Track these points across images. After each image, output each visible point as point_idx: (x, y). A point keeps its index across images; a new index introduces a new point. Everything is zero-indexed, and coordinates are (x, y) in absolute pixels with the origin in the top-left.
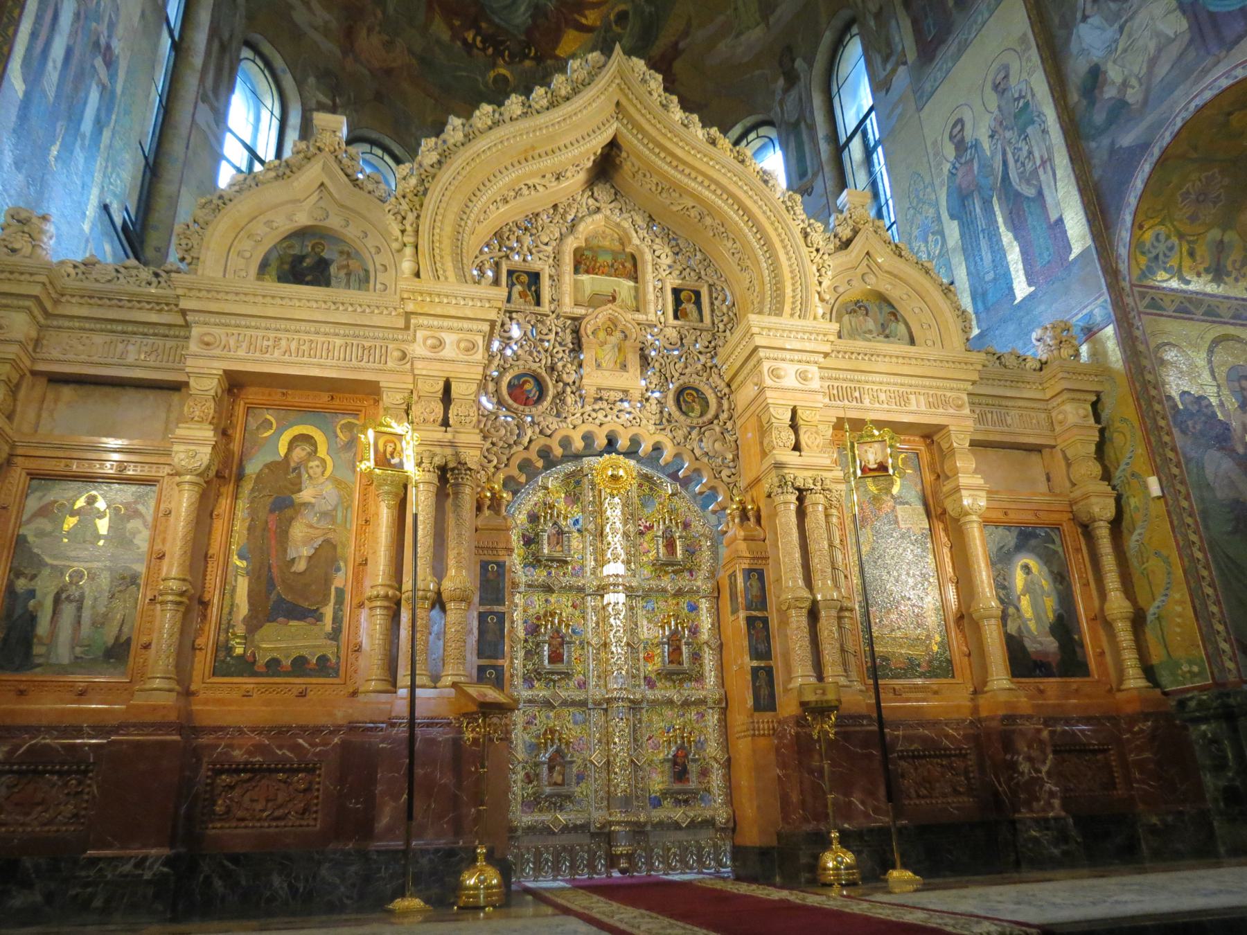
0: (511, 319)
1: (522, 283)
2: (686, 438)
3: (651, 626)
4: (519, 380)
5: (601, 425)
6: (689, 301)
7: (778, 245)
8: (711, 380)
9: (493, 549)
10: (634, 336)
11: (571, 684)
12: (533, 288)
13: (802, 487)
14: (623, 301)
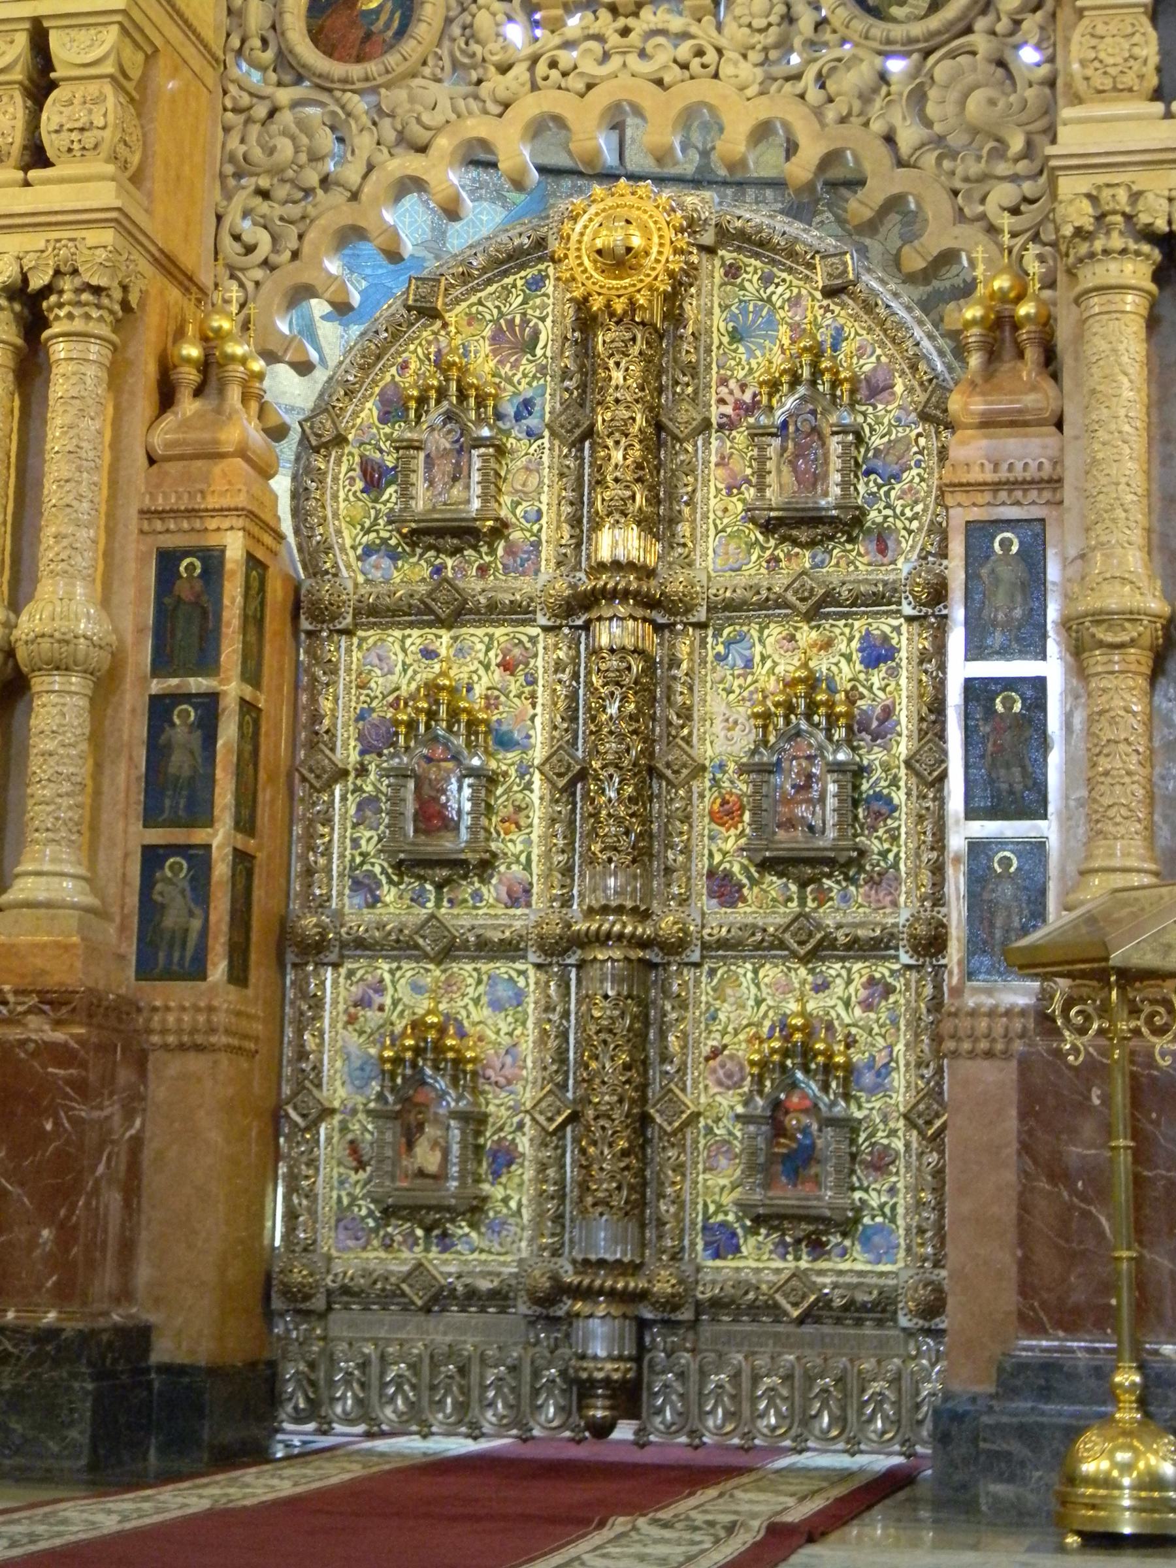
2: (866, 98)
5: (590, 87)
9: (192, 513)
11: (489, 893)
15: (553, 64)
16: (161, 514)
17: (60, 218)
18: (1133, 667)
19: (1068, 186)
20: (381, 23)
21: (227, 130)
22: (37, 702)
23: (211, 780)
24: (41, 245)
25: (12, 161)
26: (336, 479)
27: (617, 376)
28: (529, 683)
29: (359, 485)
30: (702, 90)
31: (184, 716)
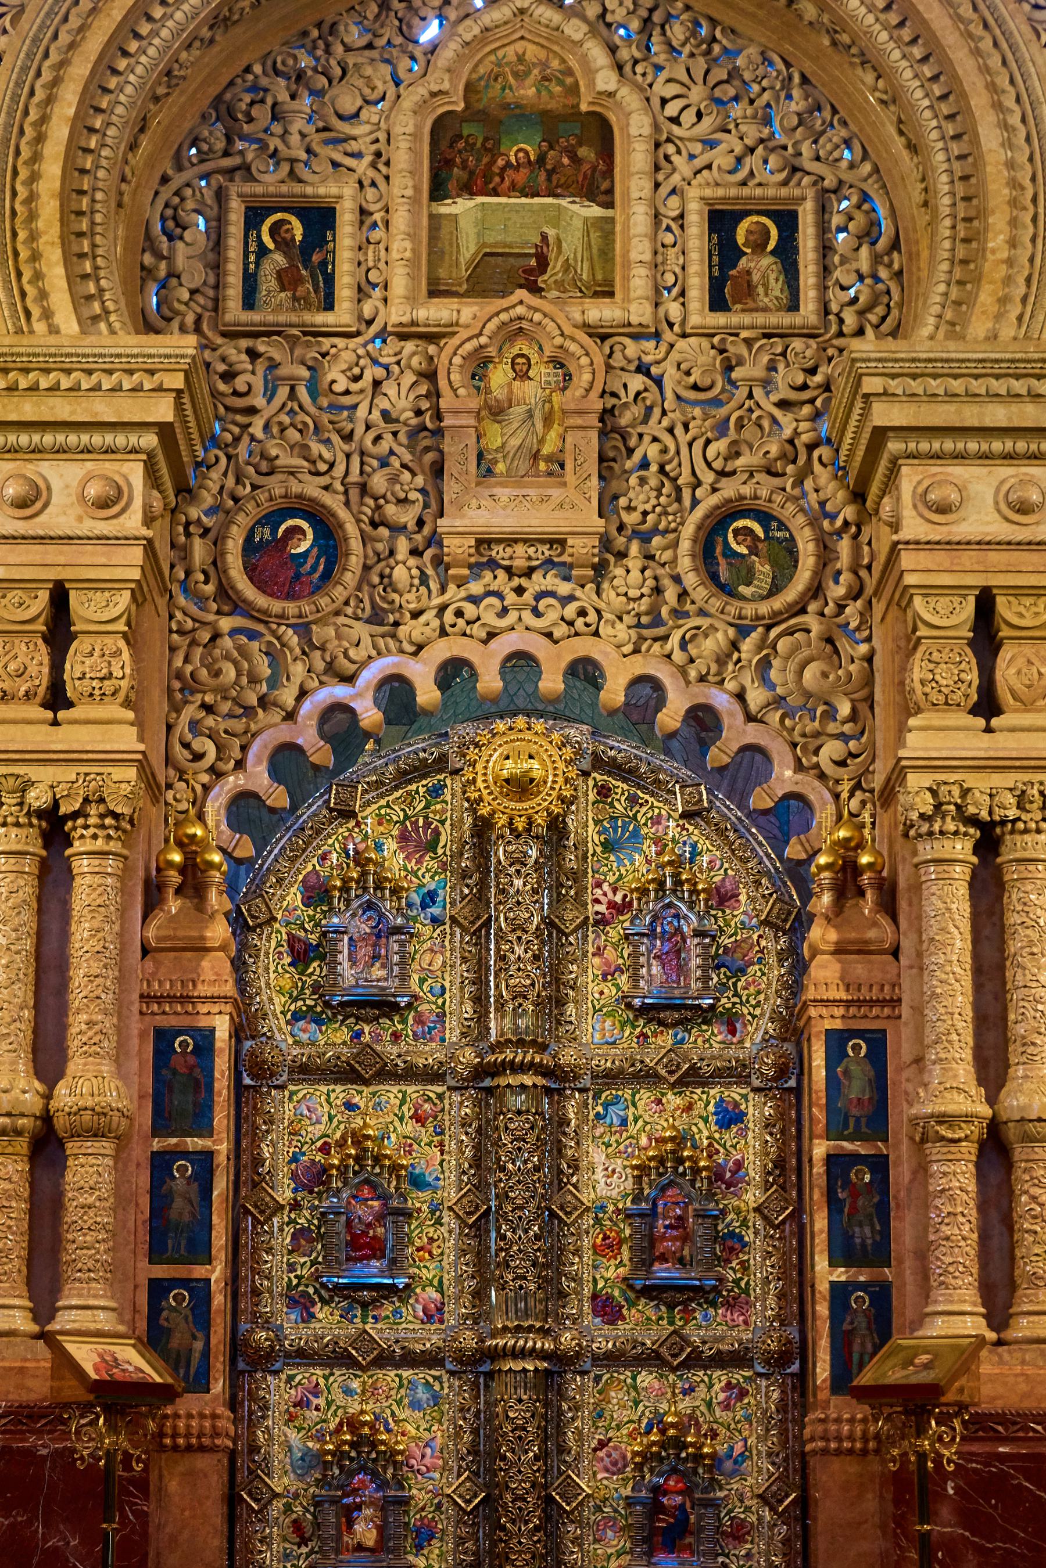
0: (253, 355)
1: (284, 244)
2: (721, 661)
3: (618, 1163)
4: (274, 530)
5: (491, 635)
6: (759, 247)
7: (979, 101)
8: (809, 484)
9: (186, 999)
10: (587, 377)
12: (316, 258)
13: (984, 815)
14: (567, 267)
15: (459, 613)
16: (159, 999)
17: (91, 756)
18: (966, 1156)
19: (914, 780)
20: (308, 566)
21: (173, 649)
22: (70, 1162)
23: (210, 1227)
24: (73, 777)
25: (38, 699)
26: (267, 954)
27: (518, 883)
28: (438, 1134)
29: (287, 960)
30: (584, 647)
31: (182, 1171)
